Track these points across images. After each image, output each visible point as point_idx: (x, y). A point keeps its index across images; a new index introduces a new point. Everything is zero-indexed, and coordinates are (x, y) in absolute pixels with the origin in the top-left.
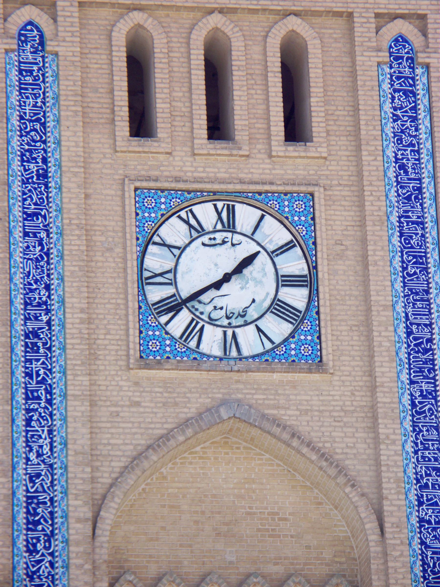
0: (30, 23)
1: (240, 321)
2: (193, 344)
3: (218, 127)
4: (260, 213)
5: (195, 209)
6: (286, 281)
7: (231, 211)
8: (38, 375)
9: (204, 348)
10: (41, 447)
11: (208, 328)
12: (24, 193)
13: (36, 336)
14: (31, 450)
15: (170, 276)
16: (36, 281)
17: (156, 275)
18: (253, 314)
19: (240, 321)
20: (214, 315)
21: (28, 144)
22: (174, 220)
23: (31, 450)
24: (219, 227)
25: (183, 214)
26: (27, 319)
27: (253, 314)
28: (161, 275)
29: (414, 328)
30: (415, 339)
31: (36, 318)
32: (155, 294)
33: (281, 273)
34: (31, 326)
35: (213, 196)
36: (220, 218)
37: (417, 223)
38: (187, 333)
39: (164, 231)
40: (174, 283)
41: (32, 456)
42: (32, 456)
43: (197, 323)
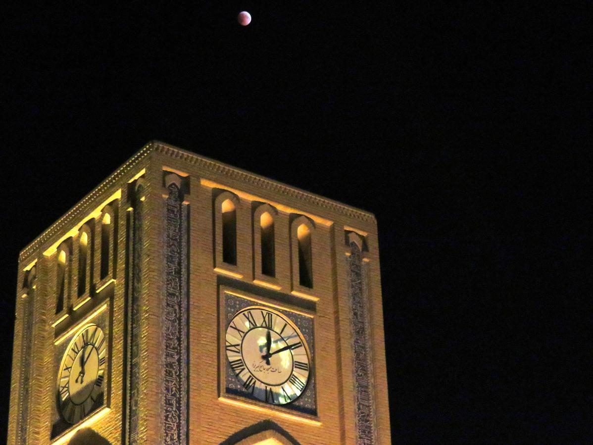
0: (174, 184)
8: (172, 391)
10: (173, 435)
12: (168, 281)
13: (171, 366)
14: (167, 436)
15: (239, 347)
16: (173, 334)
21: (170, 252)
23: (167, 436)
25: (246, 313)
26: (167, 355)
28: (234, 346)
29: (361, 406)
30: (362, 413)
31: (172, 356)
33: (295, 360)
34: (169, 360)
37: (363, 347)
40: (240, 352)
41: (168, 440)
42: (168, 440)
43: (252, 379)
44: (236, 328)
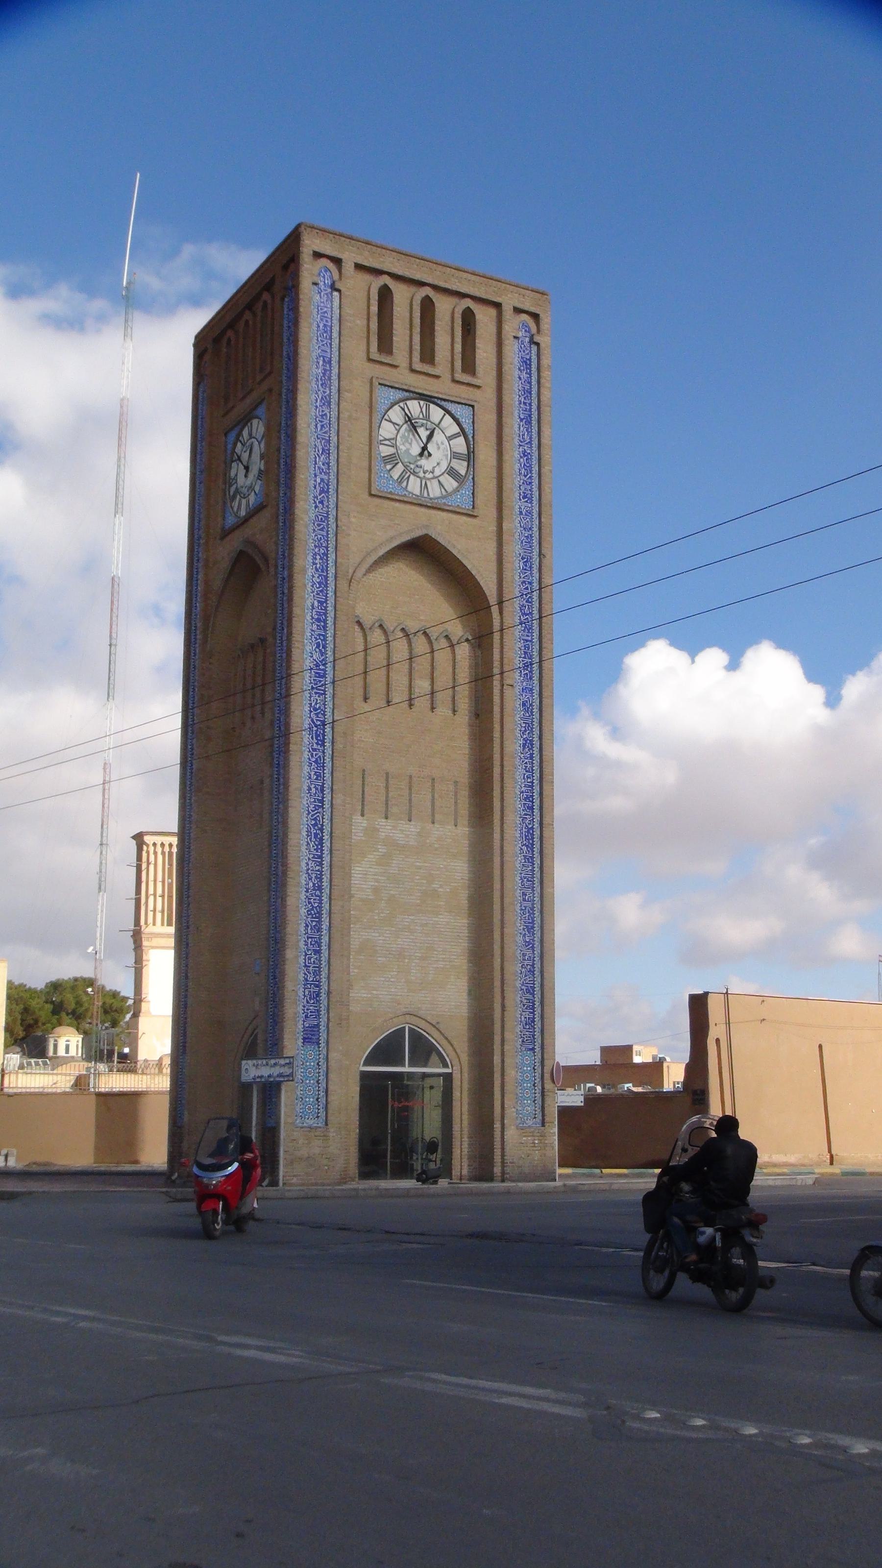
1: (431, 476)
2: (404, 484)
3: (428, 355)
4: (443, 412)
5: (408, 402)
6: (455, 455)
7: (428, 409)
9: (409, 488)
11: (412, 477)
17: (386, 440)
18: (437, 472)
19: (431, 476)
20: (417, 470)
22: (396, 407)
24: (421, 416)
25: (402, 404)
27: (437, 472)
28: (388, 440)
32: (385, 451)
35: (421, 397)
36: (422, 411)
38: (401, 477)
39: (390, 413)
44: (391, 421)
